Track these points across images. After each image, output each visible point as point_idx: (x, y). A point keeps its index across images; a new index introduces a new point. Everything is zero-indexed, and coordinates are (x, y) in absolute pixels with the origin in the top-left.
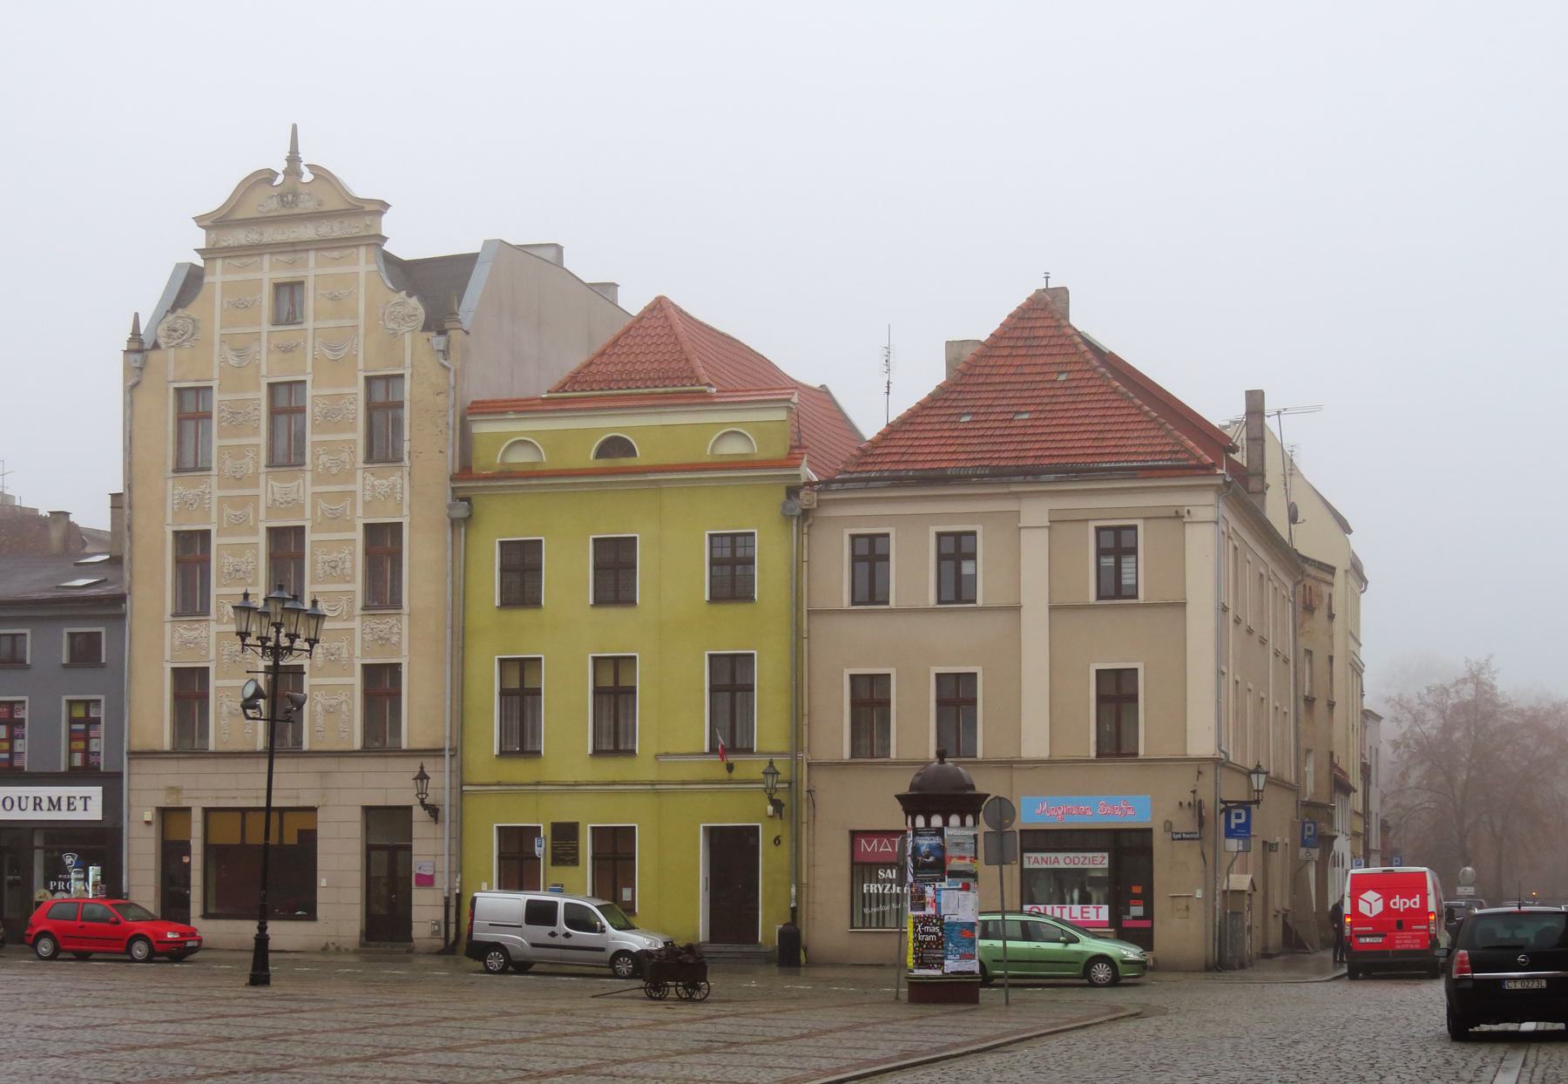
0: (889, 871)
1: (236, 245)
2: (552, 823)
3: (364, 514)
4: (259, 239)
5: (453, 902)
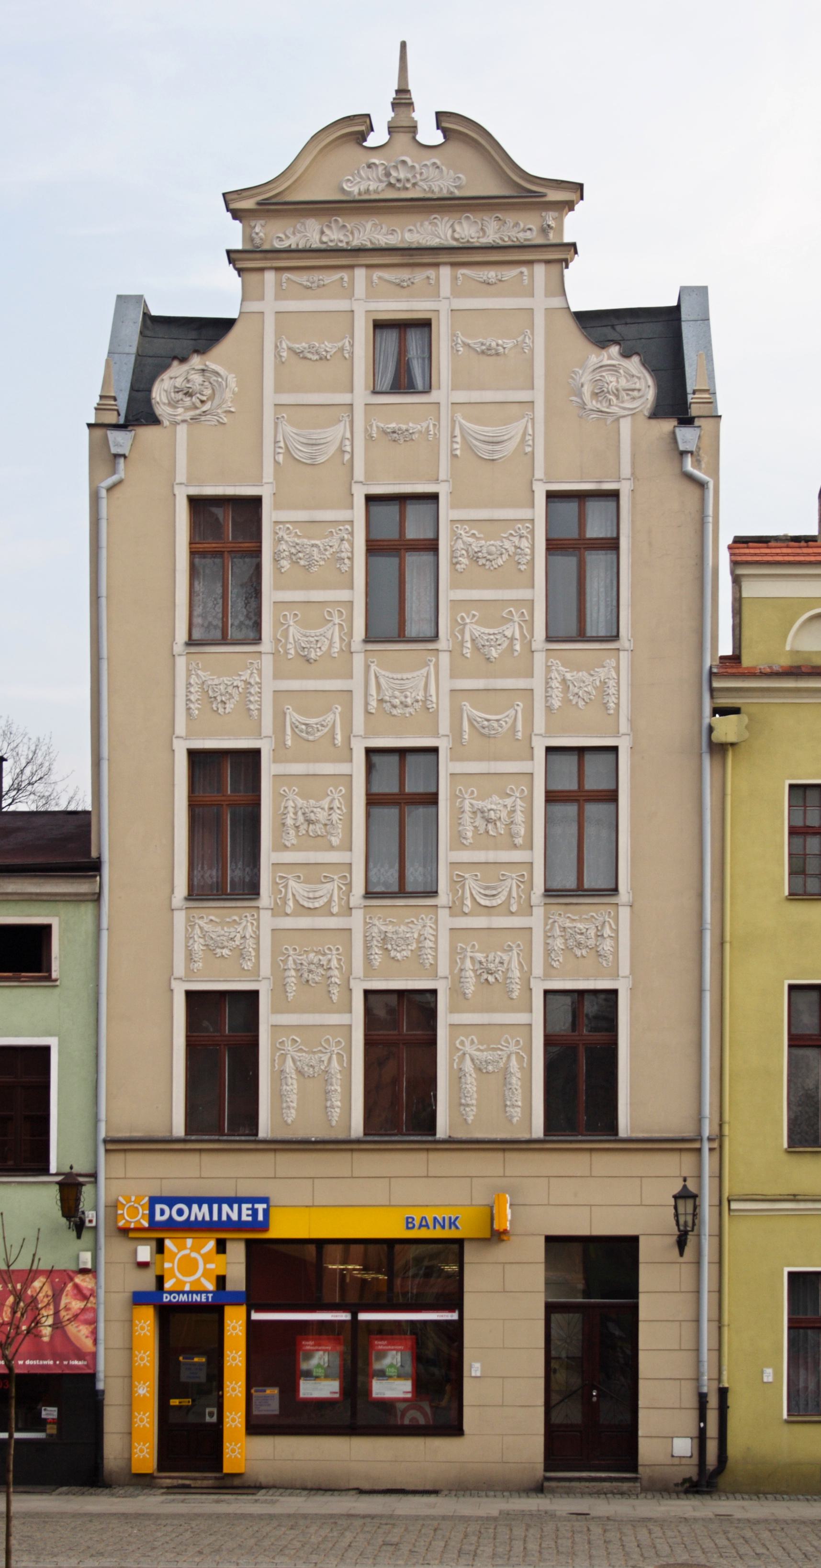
1: (300, 247)
4: (345, 240)
5: (713, 1402)
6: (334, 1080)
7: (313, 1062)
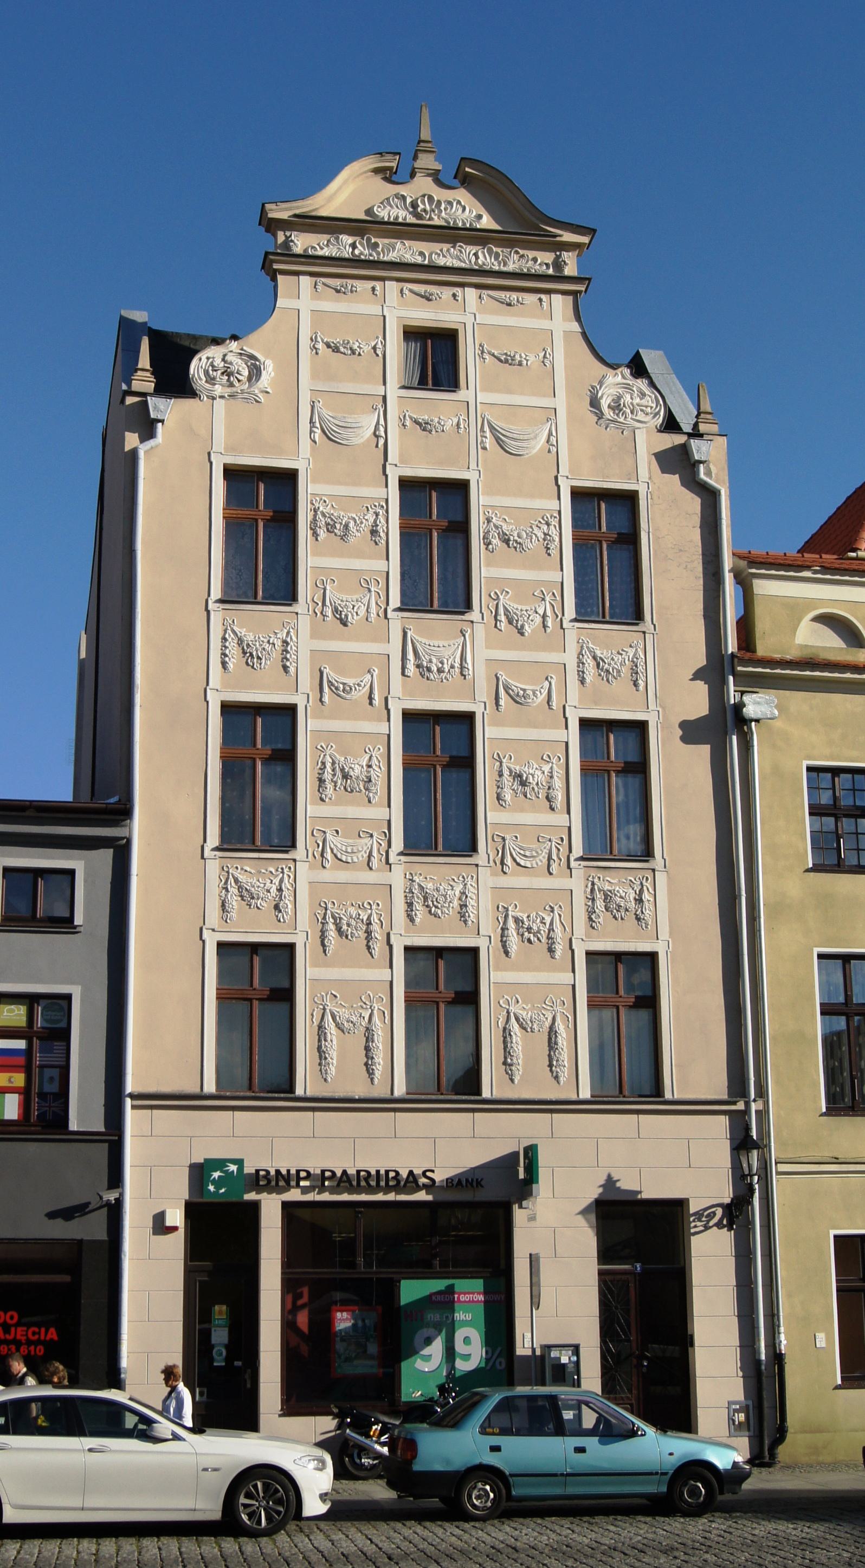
3: (580, 701)
6: (376, 1037)
7: (354, 1019)
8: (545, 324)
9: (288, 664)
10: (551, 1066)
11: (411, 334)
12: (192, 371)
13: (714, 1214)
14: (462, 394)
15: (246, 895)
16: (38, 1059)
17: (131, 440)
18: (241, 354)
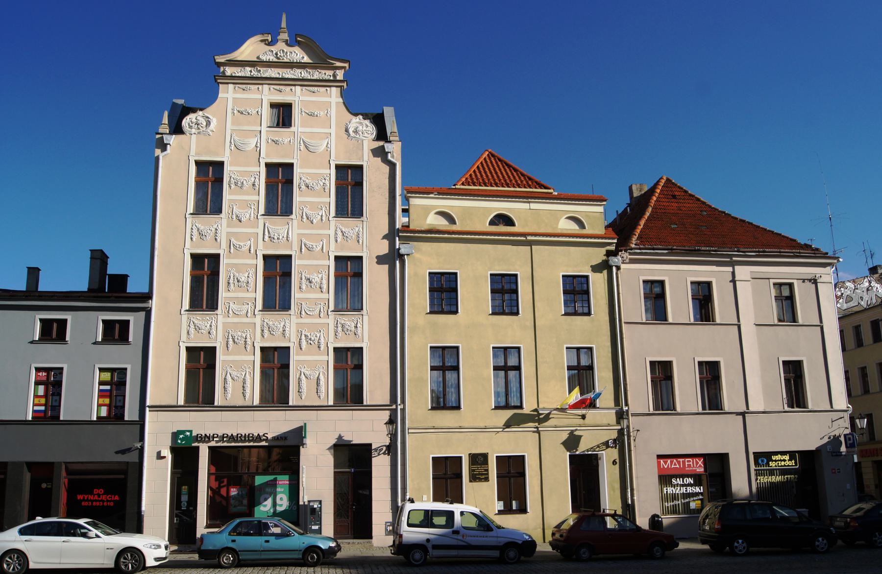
0: (678, 479)
2: (470, 454)
6: (247, 382)
7: (239, 375)
8: (328, 99)
9: (217, 238)
10: (317, 392)
11: (273, 105)
12: (183, 124)
13: (382, 449)
14: (292, 129)
15: (197, 329)
16: (114, 393)
17: (158, 152)
18: (203, 116)
